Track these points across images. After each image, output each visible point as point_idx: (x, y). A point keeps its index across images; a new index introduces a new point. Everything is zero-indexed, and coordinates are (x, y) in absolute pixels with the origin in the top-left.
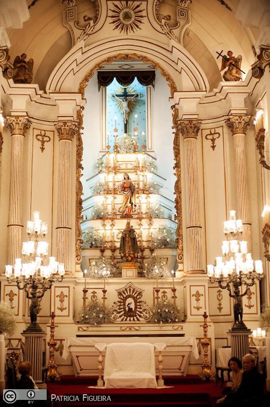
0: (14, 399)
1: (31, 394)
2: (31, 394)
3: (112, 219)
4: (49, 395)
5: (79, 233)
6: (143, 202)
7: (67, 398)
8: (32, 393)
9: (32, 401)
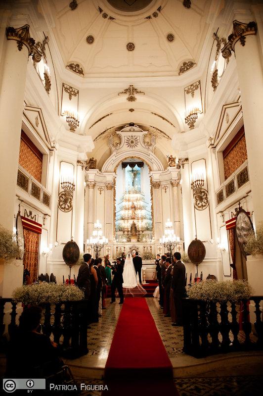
3: (128, 220)
5: (115, 225)
6: (139, 213)
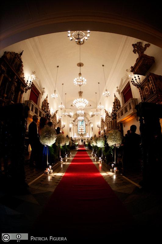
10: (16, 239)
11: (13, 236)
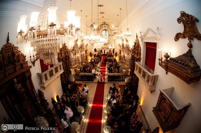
0: (7, 129)
1: (15, 127)
2: (15, 127)
4: (24, 128)
7: (33, 129)
8: (16, 126)
9: (16, 130)
10: (13, 129)
11: (11, 127)
